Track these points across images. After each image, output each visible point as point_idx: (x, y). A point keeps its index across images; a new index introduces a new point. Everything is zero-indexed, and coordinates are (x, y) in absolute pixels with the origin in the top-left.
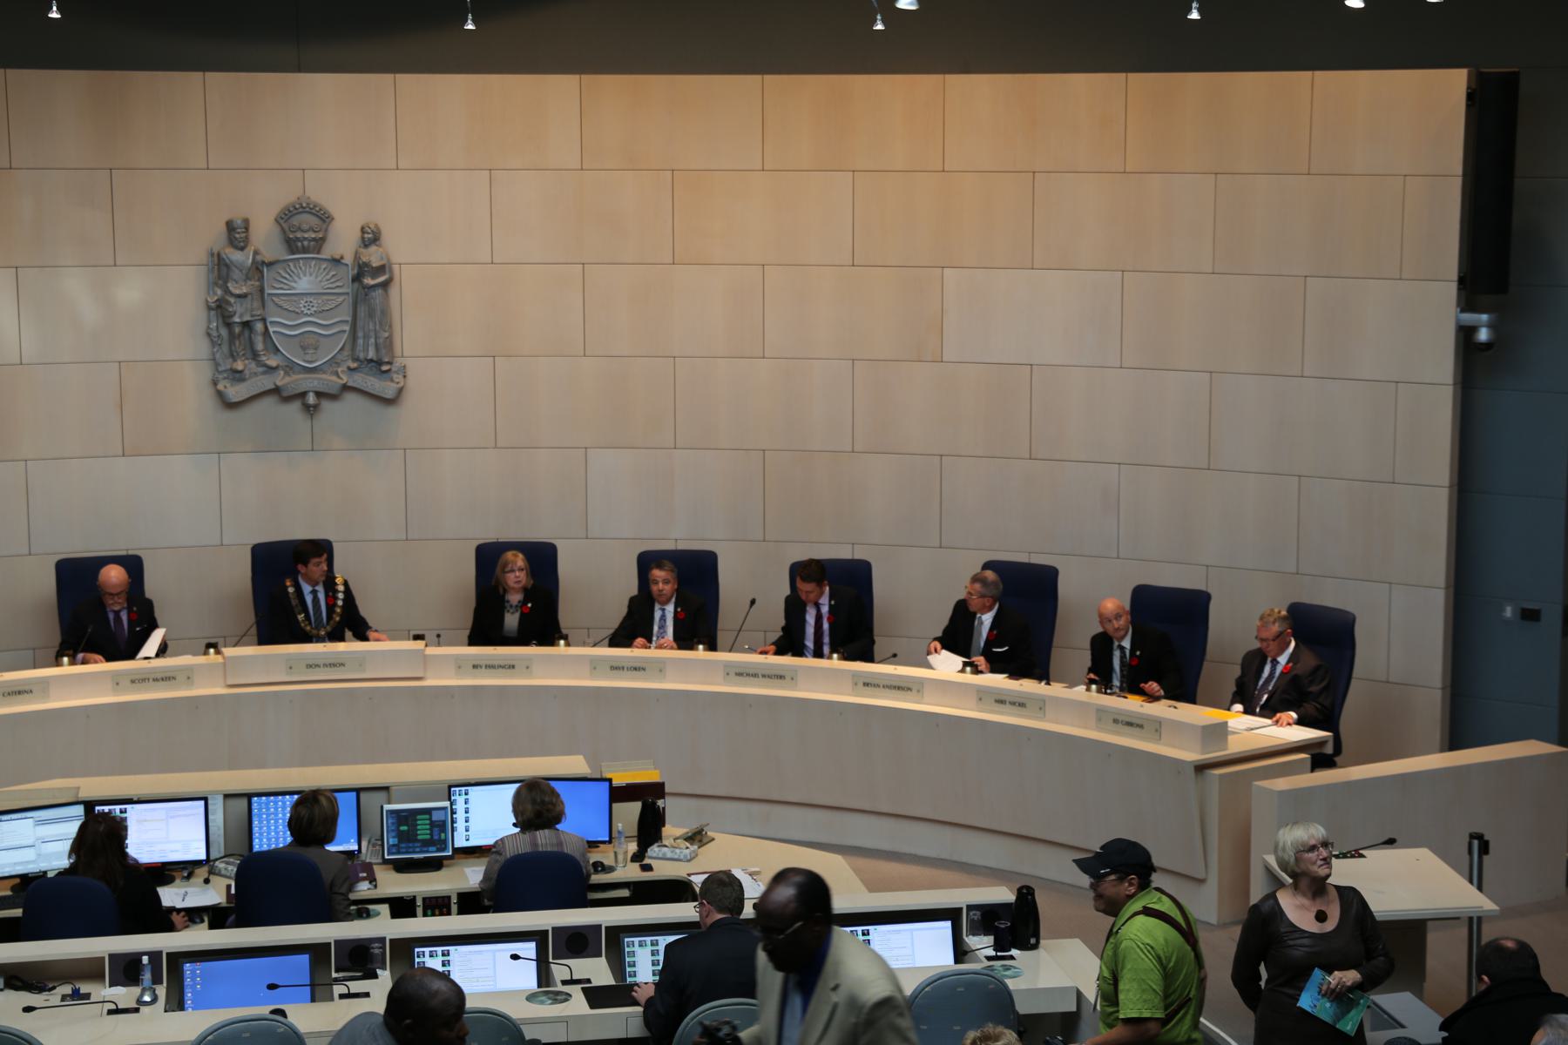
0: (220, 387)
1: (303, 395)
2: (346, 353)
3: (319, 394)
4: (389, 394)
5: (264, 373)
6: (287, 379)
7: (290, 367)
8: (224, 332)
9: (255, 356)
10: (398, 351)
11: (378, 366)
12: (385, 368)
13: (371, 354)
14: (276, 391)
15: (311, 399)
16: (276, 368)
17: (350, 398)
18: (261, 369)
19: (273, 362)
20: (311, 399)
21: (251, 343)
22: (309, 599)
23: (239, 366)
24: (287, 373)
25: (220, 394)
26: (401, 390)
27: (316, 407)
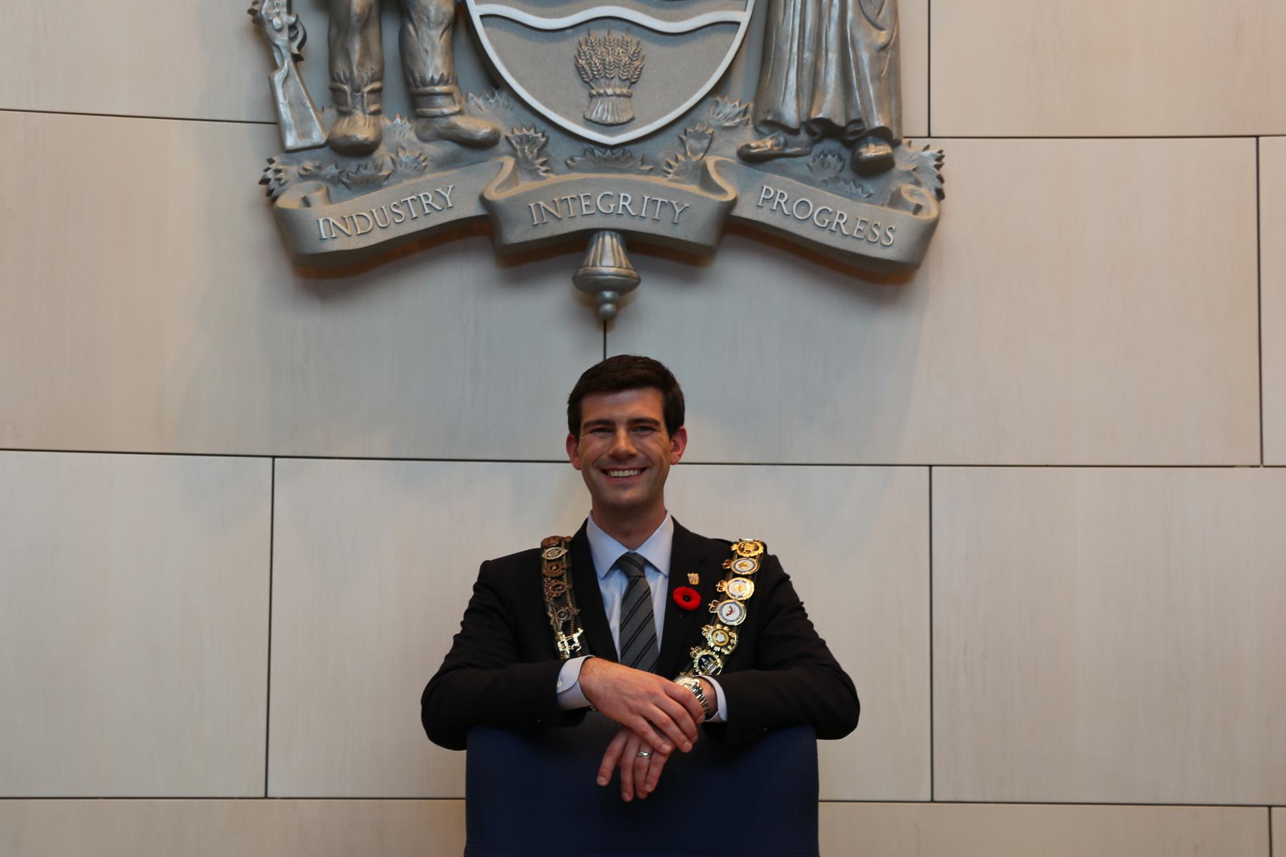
0: (288, 201)
1: (580, 242)
2: (729, 107)
3: (635, 243)
4: (890, 247)
5: (446, 163)
6: (526, 184)
7: (542, 142)
8: (316, 29)
9: (416, 99)
10: (913, 122)
11: (855, 148)
12: (872, 151)
13: (829, 107)
14: (477, 233)
15: (608, 259)
16: (479, 146)
17: (746, 281)
18: (435, 150)
19: (479, 126)
20: (608, 259)
21: (406, 55)
22: (613, 591)
23: (361, 129)
24: (524, 166)
25: (285, 228)
26: (929, 231)
27: (624, 288)
